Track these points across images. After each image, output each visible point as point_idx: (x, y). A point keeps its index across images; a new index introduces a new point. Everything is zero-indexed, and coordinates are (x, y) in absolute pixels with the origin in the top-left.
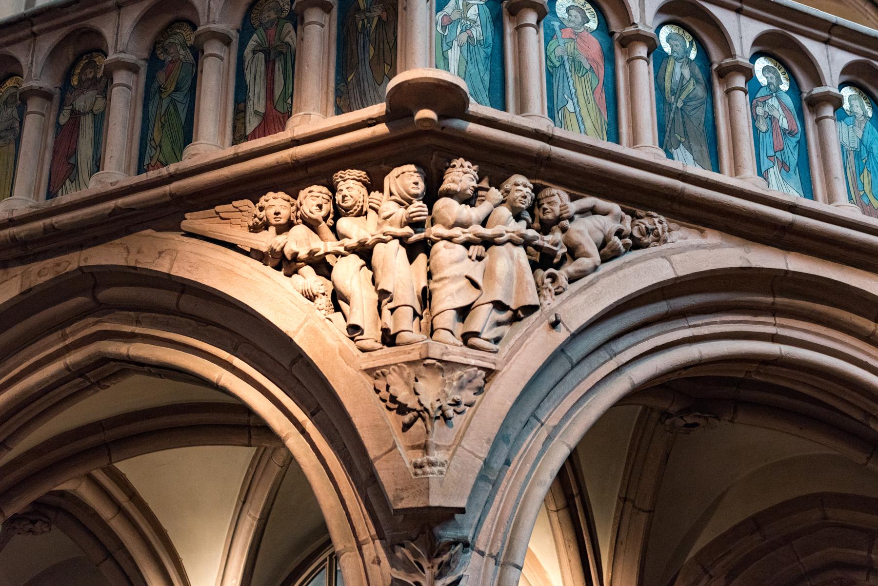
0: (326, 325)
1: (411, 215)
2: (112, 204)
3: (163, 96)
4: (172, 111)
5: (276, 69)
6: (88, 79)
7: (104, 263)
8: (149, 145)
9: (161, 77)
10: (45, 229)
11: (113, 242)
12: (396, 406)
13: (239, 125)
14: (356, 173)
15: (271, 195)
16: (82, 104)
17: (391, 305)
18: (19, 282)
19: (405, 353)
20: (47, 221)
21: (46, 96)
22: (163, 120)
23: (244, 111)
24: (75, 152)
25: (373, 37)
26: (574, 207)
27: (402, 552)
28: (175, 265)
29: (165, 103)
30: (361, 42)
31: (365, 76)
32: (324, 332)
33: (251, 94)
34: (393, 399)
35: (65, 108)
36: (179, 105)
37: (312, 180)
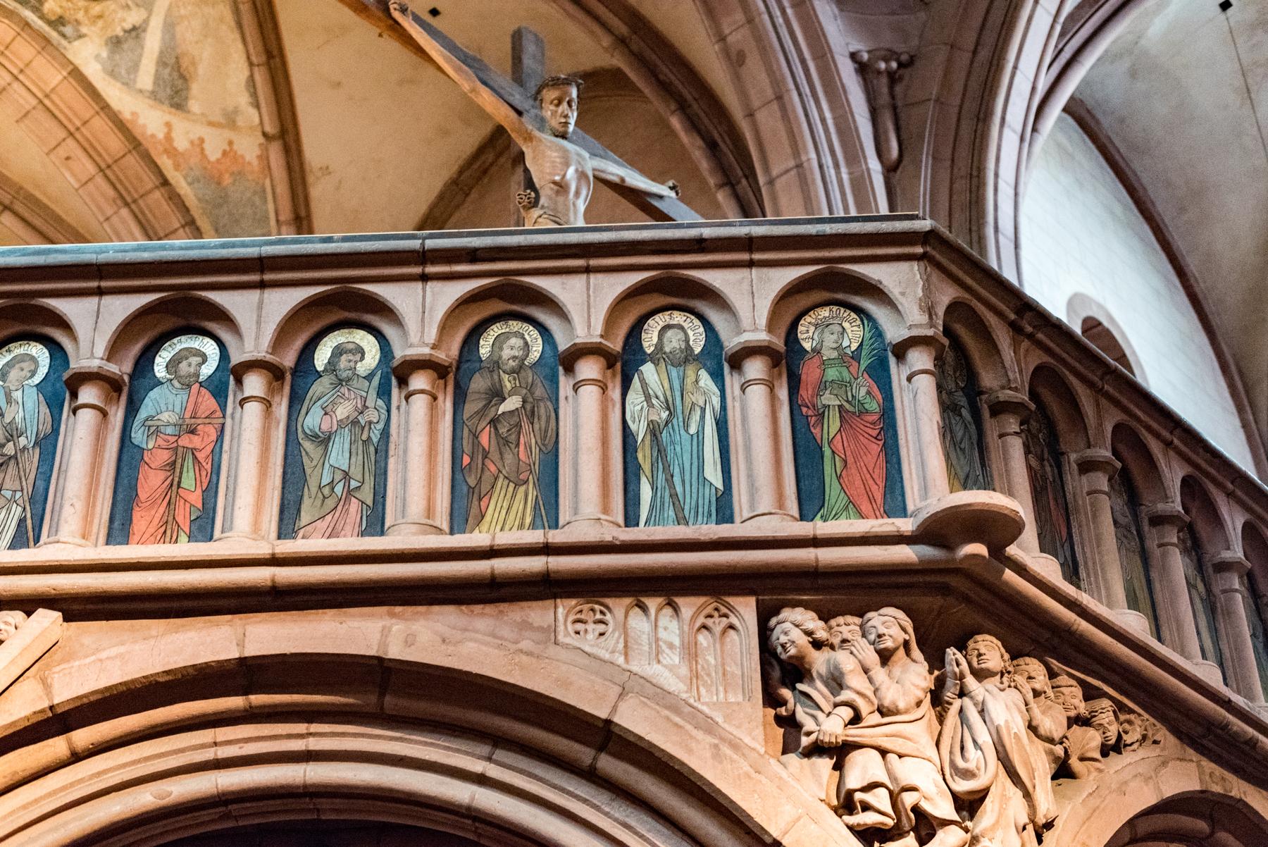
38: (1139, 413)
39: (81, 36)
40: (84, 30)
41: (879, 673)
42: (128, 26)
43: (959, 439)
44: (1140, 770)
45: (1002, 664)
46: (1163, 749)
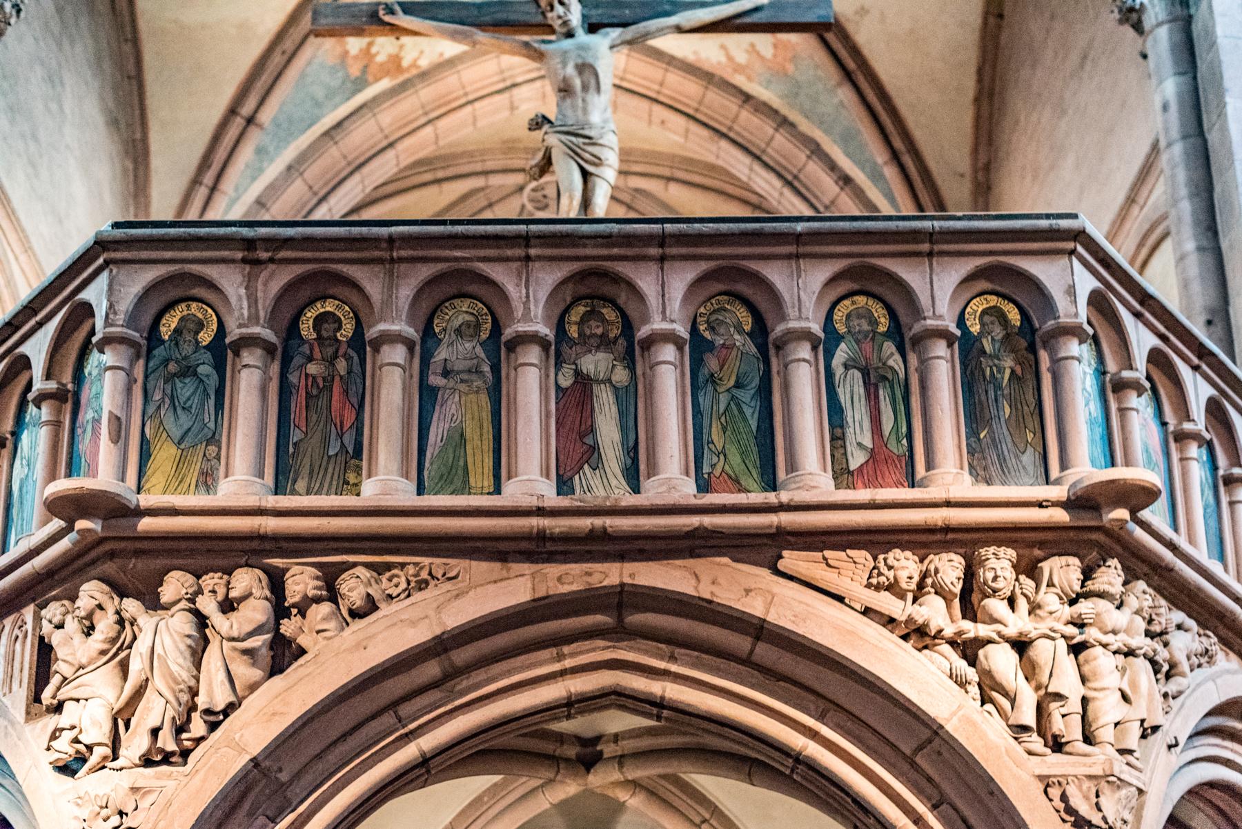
0: (984, 717)
1: (1083, 616)
3: (720, 389)
4: (736, 412)
5: (881, 397)
6: (595, 335)
7: (660, 585)
8: (706, 447)
9: (712, 363)
11: (671, 561)
12: (1073, 819)
13: (837, 455)
14: (1011, 553)
15: (897, 552)
16: (591, 367)
17: (1064, 711)
18: (529, 585)
19: (1085, 765)
21: (544, 344)
22: (723, 419)
23: (843, 438)
24: (592, 430)
25: (1006, 392)
28: (772, 610)
29: (724, 399)
30: (991, 393)
31: (1001, 436)
32: (983, 726)
33: (850, 420)
34: (1070, 810)
35: (564, 365)
36: (743, 406)
37: (946, 546)
38: (458, 254)
43: (182, 400)
44: (403, 617)
45: (184, 591)
46: (463, 581)
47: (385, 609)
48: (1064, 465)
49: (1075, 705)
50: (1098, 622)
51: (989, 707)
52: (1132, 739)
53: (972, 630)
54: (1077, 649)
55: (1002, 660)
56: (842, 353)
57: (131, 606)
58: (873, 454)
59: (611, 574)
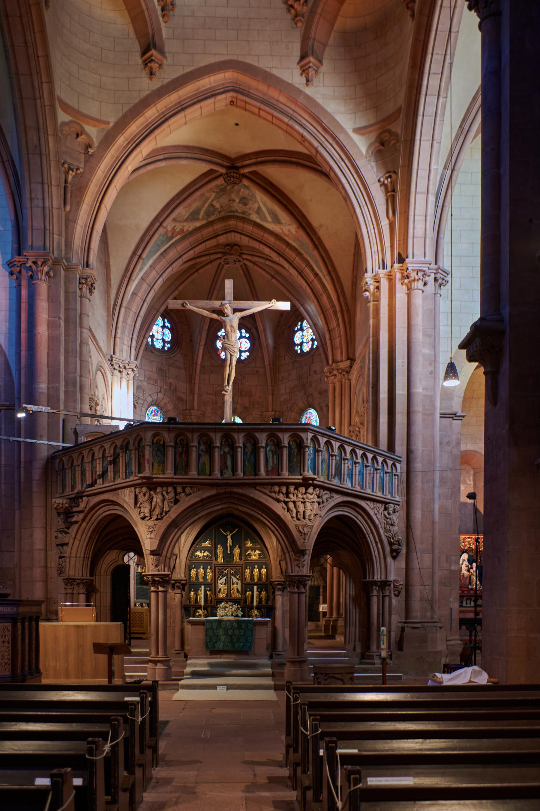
2: (242, 481)
9: (247, 450)
10: (226, 483)
14: (294, 487)
20: (227, 481)
21: (218, 447)
26: (324, 493)
27: (298, 555)
29: (248, 457)
34: (299, 530)
39: (250, 214)
40: (250, 212)
41: (143, 497)
42: (257, 208)
47: (193, 495)
48: (304, 471)
49: (302, 513)
50: (307, 498)
51: (288, 513)
52: (312, 517)
53: (286, 500)
54: (304, 503)
55: (291, 505)
56: (268, 448)
57: (152, 492)
58: (272, 468)
59: (229, 489)
